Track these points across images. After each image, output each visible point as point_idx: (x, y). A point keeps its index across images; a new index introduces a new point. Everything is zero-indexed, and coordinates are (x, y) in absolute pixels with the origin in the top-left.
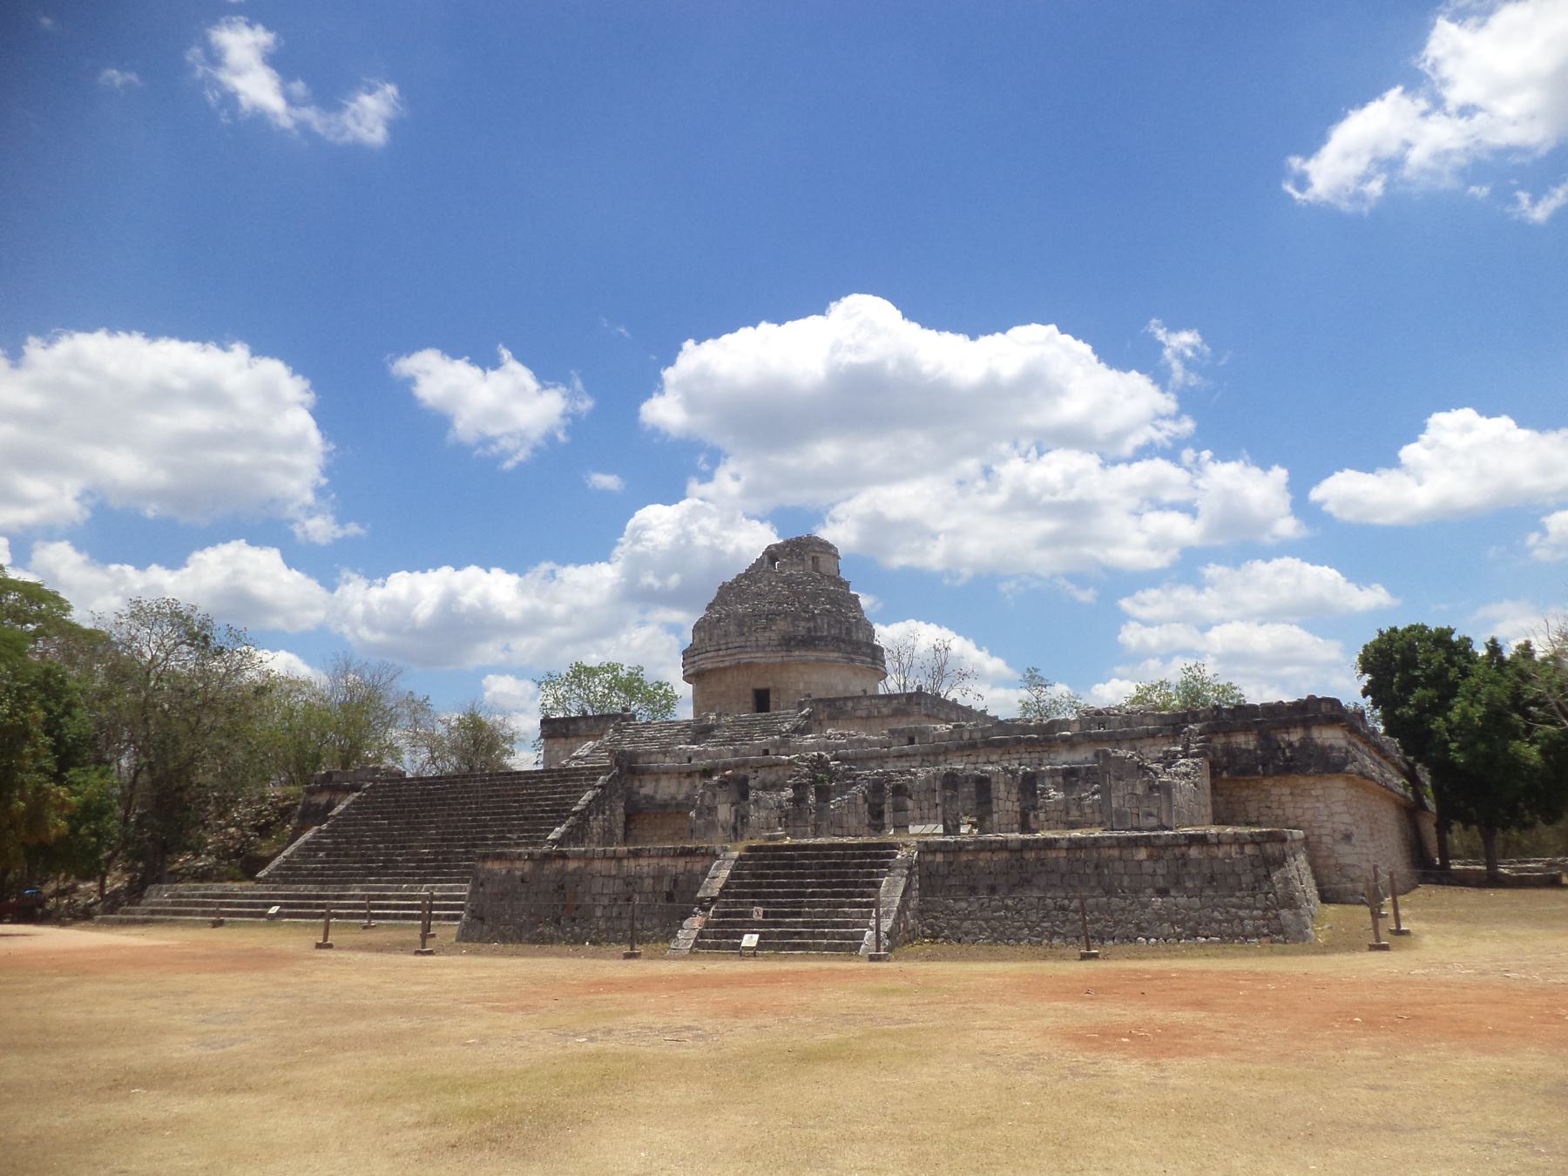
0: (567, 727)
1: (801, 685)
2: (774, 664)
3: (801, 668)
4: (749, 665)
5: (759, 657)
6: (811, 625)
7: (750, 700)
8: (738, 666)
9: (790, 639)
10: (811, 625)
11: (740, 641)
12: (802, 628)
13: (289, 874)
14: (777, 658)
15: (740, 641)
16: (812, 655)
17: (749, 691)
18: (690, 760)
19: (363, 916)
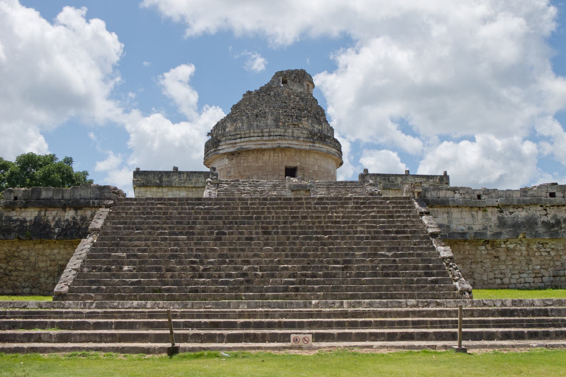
0: (161, 180)
1: (316, 167)
2: (300, 150)
3: (316, 156)
4: (283, 149)
5: (294, 144)
6: (320, 128)
7: (283, 173)
8: (274, 149)
9: (315, 134)
10: (320, 128)
11: (280, 131)
12: (317, 127)
13: (84, 286)
14: (306, 146)
15: (280, 131)
16: (325, 148)
17: (284, 168)
18: (479, 197)
19: (453, 336)
